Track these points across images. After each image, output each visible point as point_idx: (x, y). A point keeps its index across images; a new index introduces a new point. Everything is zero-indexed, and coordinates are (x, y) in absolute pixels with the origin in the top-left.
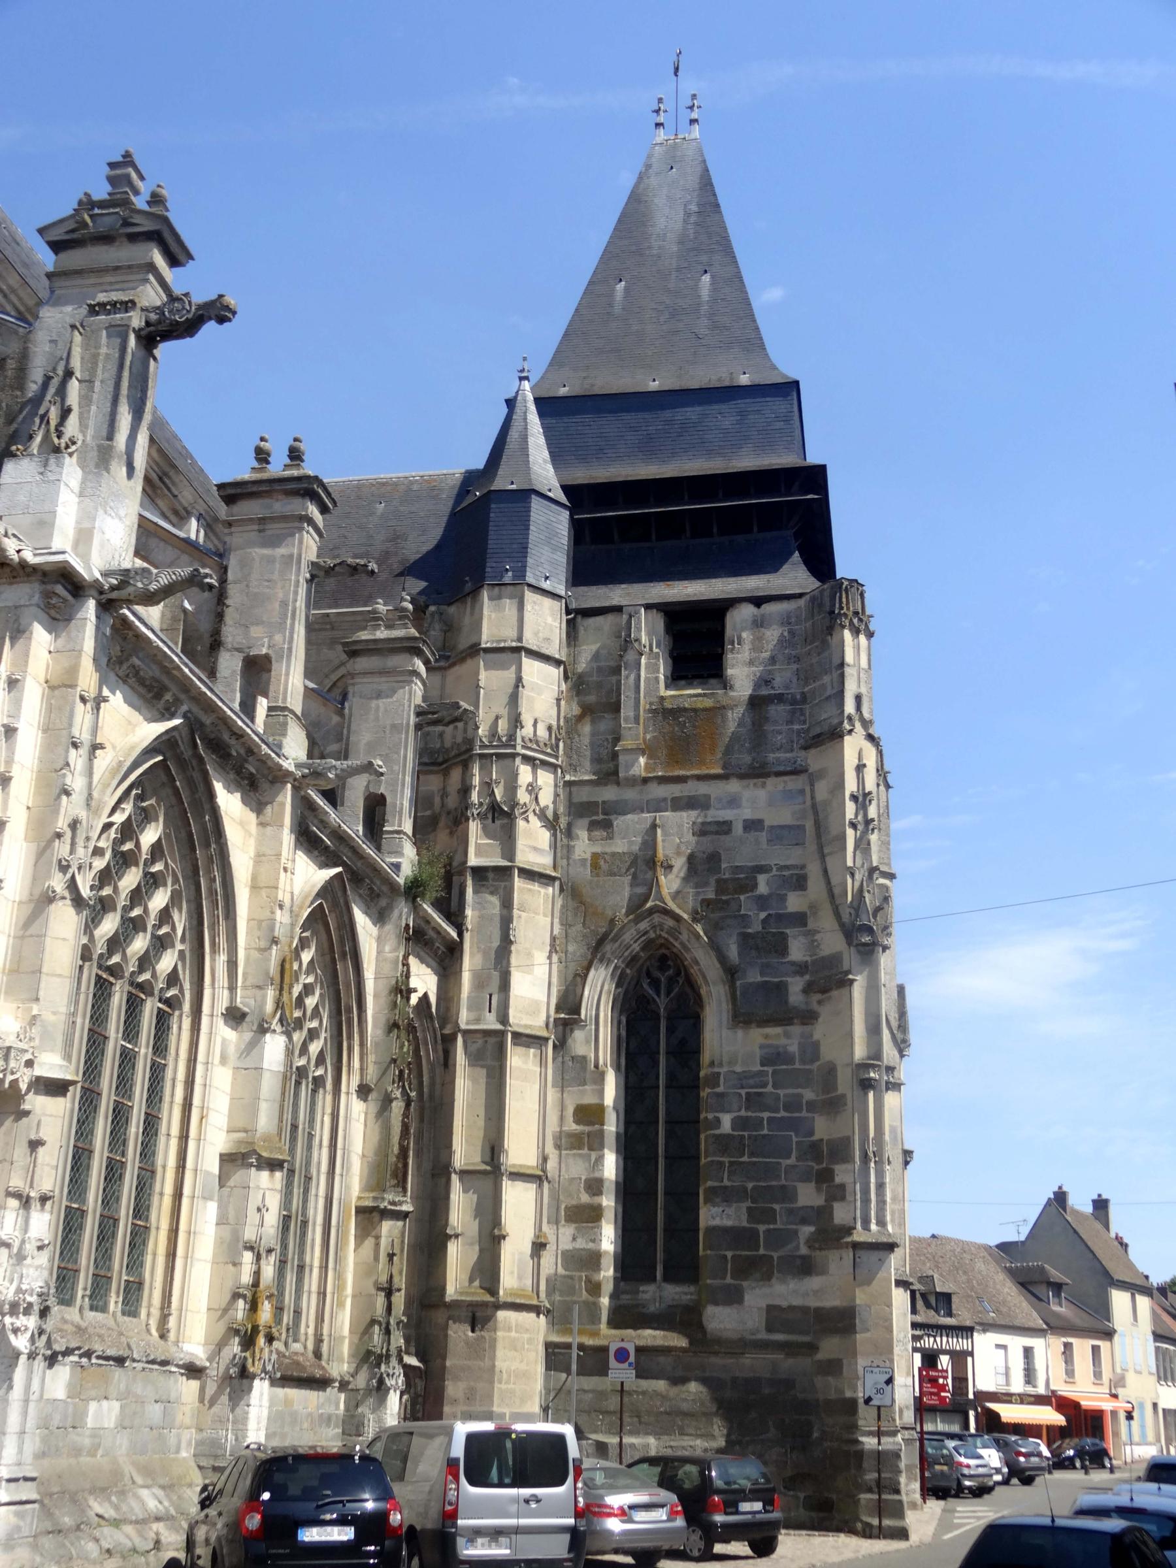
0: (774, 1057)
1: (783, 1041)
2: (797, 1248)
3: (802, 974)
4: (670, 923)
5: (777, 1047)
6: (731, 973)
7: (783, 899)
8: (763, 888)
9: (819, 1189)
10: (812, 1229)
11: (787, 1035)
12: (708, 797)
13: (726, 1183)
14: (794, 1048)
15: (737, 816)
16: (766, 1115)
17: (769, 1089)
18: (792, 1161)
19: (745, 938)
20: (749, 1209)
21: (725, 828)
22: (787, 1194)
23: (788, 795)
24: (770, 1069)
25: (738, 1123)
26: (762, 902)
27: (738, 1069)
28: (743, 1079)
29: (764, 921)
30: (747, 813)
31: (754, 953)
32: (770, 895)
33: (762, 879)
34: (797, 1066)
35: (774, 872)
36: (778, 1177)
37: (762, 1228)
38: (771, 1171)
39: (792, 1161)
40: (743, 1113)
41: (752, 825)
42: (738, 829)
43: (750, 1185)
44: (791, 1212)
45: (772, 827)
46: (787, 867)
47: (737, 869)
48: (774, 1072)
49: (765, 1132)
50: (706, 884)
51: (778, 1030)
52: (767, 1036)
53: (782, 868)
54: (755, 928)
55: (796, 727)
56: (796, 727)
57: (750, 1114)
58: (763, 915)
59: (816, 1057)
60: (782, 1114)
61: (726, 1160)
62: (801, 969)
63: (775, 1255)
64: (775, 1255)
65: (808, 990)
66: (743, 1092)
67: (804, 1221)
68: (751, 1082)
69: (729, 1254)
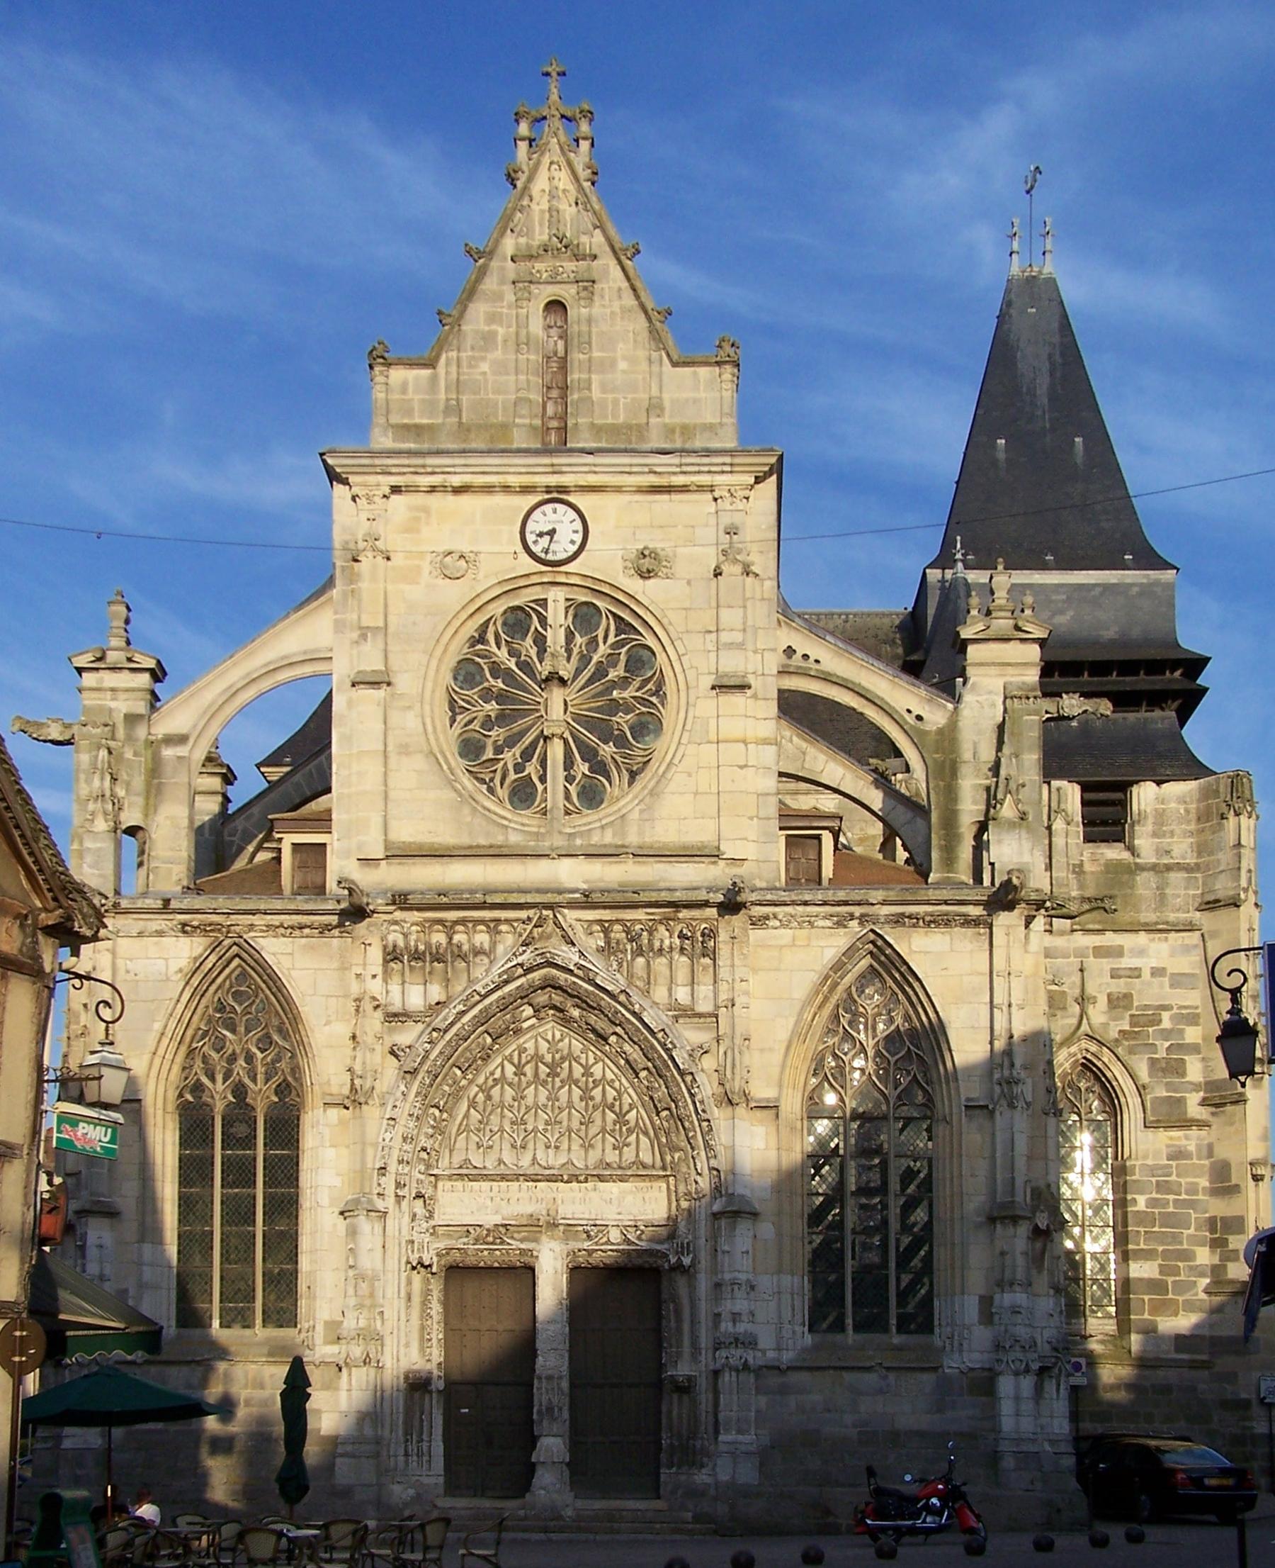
0: (1178, 1154)
1: (1184, 1142)
2: (1197, 1294)
3: (1198, 1091)
4: (1094, 1048)
5: (1179, 1147)
6: (1141, 1089)
7: (1181, 1032)
8: (1166, 1023)
9: (1212, 1252)
10: (1208, 1281)
11: (1187, 1138)
12: (1121, 947)
13: (1142, 1246)
14: (1192, 1148)
15: (1146, 964)
16: (1171, 1197)
17: (1174, 1178)
18: (1192, 1231)
19: (1153, 1062)
20: (1160, 1265)
21: (1136, 973)
22: (1187, 1256)
23: (1187, 949)
24: (1173, 1163)
25: (1152, 1203)
26: (1166, 1034)
27: (1150, 1162)
28: (1152, 1170)
29: (1168, 1049)
30: (1154, 963)
31: (1160, 1074)
32: (1172, 1030)
33: (1166, 1016)
34: (1195, 1161)
35: (1175, 1011)
36: (1181, 1243)
37: (1170, 1280)
38: (1176, 1238)
39: (1192, 1231)
40: (1154, 1195)
41: (1157, 972)
42: (1146, 974)
43: (1160, 1249)
44: (1191, 1268)
45: (1172, 974)
46: (1185, 1007)
47: (1147, 1007)
48: (1177, 1166)
49: (1171, 1210)
50: (1122, 1018)
51: (1180, 1133)
52: (1171, 1138)
53: (1181, 1007)
54: (1161, 1054)
55: (1192, 892)
56: (1192, 892)
57: (1159, 1196)
58: (1167, 1044)
59: (1210, 1154)
60: (1184, 1196)
61: (1142, 1230)
62: (1196, 1087)
63: (1181, 1299)
64: (1181, 1299)
65: (1204, 1102)
66: (1154, 1180)
67: (1202, 1275)
68: (1160, 1172)
69: (1146, 1298)
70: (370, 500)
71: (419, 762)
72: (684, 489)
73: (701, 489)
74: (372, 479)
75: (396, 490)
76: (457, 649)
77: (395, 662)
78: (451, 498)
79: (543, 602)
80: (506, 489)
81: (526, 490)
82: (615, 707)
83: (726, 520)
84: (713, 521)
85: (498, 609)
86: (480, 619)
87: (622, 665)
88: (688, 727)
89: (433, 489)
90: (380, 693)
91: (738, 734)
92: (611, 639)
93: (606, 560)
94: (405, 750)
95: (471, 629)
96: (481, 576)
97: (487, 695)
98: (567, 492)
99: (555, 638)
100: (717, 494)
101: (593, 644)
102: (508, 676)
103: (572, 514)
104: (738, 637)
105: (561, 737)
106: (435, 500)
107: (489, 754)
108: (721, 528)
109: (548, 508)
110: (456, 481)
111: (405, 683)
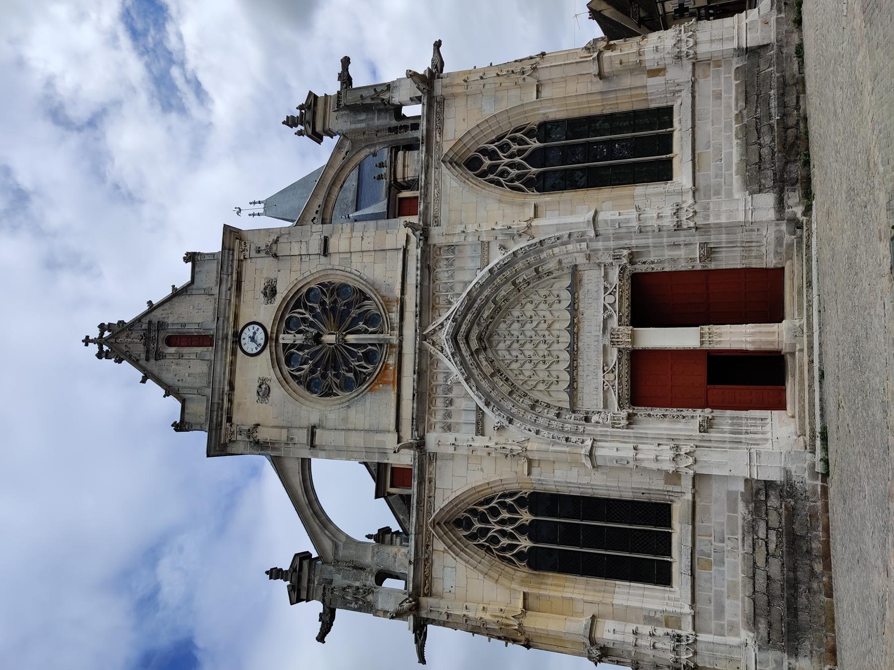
70: (232, 433)
71: (352, 412)
72: (239, 274)
73: (240, 266)
74: (223, 431)
75: (229, 419)
76: (301, 389)
77: (305, 423)
78: (236, 392)
79: (285, 345)
80: (233, 363)
81: (234, 353)
82: (333, 309)
83: (253, 254)
84: (254, 260)
85: (285, 368)
86: (290, 378)
87: (314, 305)
88: (343, 268)
89: (230, 401)
90: (318, 431)
91: (347, 241)
92: (303, 311)
93: (266, 313)
94: (345, 420)
95: (294, 383)
96: (269, 377)
97: (324, 376)
98: (237, 332)
99: (300, 339)
100: (242, 258)
101: (304, 320)
102: (316, 365)
103: (246, 330)
104: (304, 244)
105: (345, 335)
106: (236, 402)
107: (351, 375)
108: (257, 255)
109: (243, 342)
110: (227, 388)
111: (314, 419)
